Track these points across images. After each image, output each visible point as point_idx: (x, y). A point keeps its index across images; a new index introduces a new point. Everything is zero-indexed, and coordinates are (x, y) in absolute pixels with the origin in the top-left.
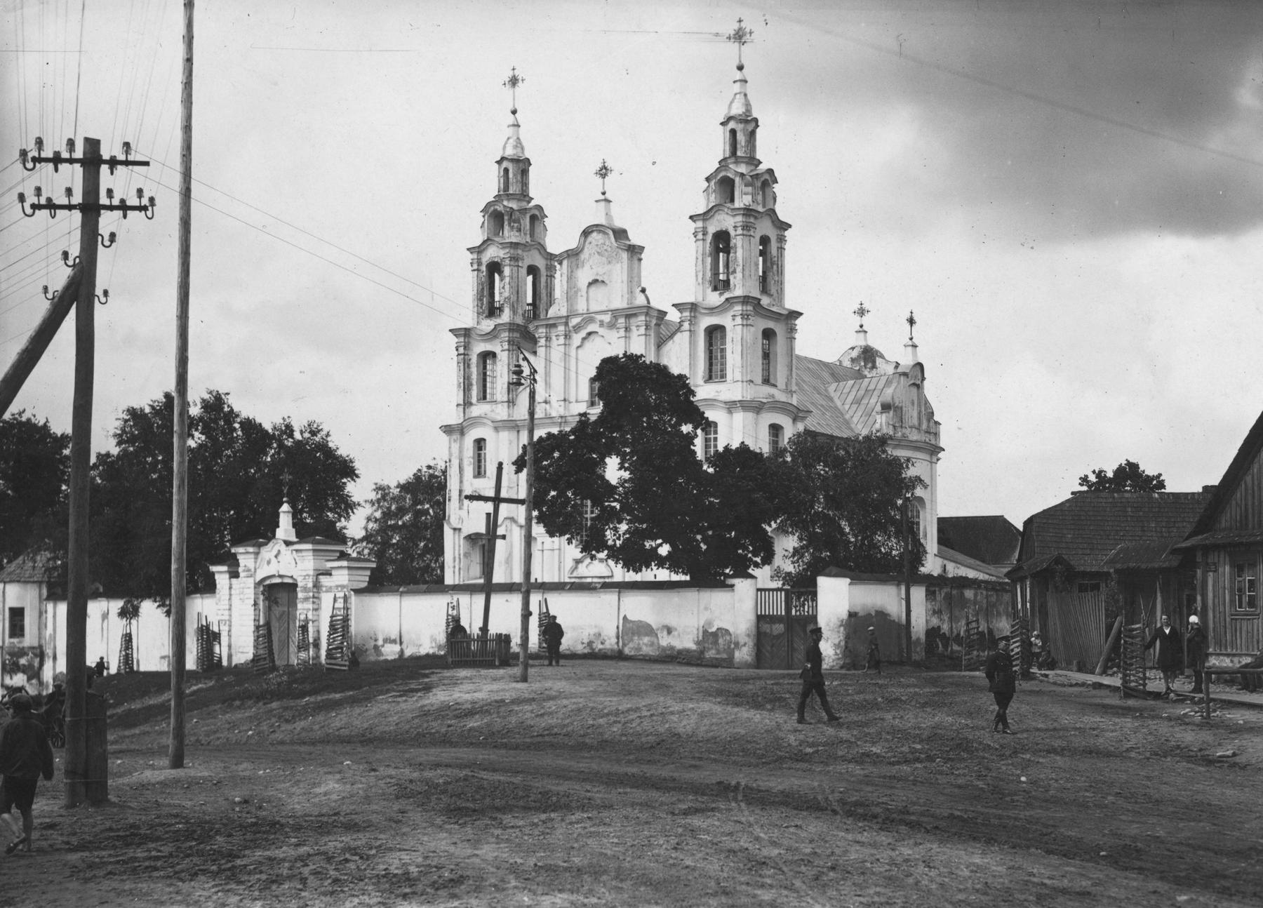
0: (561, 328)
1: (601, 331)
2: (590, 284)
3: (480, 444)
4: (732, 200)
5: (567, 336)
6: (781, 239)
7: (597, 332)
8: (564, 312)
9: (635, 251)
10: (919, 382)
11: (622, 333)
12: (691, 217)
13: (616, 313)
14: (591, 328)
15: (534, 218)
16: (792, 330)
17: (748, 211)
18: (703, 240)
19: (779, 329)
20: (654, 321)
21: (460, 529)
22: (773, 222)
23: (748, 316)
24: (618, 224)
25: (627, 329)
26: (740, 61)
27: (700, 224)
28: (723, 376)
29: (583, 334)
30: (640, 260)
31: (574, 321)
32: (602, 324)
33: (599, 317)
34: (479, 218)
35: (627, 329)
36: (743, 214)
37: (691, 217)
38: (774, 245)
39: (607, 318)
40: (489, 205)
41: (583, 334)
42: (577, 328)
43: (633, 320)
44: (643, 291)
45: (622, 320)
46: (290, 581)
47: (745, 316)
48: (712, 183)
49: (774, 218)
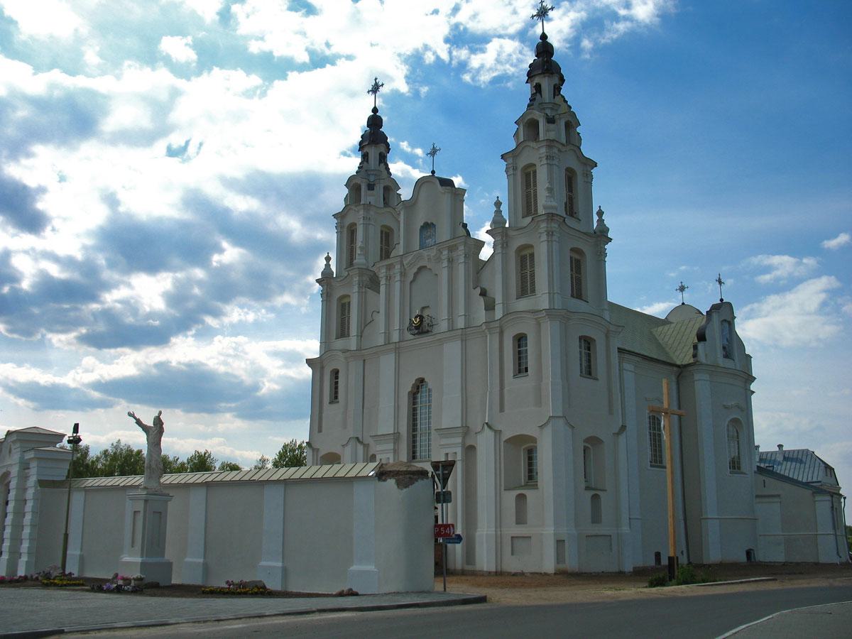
0: (398, 267)
5: (403, 274)
6: (589, 178)
7: (425, 267)
10: (729, 320)
11: (445, 264)
17: (551, 143)
21: (318, 449)
23: (552, 233)
25: (451, 261)
28: (533, 291)
38: (580, 179)
41: (415, 270)
47: (550, 234)
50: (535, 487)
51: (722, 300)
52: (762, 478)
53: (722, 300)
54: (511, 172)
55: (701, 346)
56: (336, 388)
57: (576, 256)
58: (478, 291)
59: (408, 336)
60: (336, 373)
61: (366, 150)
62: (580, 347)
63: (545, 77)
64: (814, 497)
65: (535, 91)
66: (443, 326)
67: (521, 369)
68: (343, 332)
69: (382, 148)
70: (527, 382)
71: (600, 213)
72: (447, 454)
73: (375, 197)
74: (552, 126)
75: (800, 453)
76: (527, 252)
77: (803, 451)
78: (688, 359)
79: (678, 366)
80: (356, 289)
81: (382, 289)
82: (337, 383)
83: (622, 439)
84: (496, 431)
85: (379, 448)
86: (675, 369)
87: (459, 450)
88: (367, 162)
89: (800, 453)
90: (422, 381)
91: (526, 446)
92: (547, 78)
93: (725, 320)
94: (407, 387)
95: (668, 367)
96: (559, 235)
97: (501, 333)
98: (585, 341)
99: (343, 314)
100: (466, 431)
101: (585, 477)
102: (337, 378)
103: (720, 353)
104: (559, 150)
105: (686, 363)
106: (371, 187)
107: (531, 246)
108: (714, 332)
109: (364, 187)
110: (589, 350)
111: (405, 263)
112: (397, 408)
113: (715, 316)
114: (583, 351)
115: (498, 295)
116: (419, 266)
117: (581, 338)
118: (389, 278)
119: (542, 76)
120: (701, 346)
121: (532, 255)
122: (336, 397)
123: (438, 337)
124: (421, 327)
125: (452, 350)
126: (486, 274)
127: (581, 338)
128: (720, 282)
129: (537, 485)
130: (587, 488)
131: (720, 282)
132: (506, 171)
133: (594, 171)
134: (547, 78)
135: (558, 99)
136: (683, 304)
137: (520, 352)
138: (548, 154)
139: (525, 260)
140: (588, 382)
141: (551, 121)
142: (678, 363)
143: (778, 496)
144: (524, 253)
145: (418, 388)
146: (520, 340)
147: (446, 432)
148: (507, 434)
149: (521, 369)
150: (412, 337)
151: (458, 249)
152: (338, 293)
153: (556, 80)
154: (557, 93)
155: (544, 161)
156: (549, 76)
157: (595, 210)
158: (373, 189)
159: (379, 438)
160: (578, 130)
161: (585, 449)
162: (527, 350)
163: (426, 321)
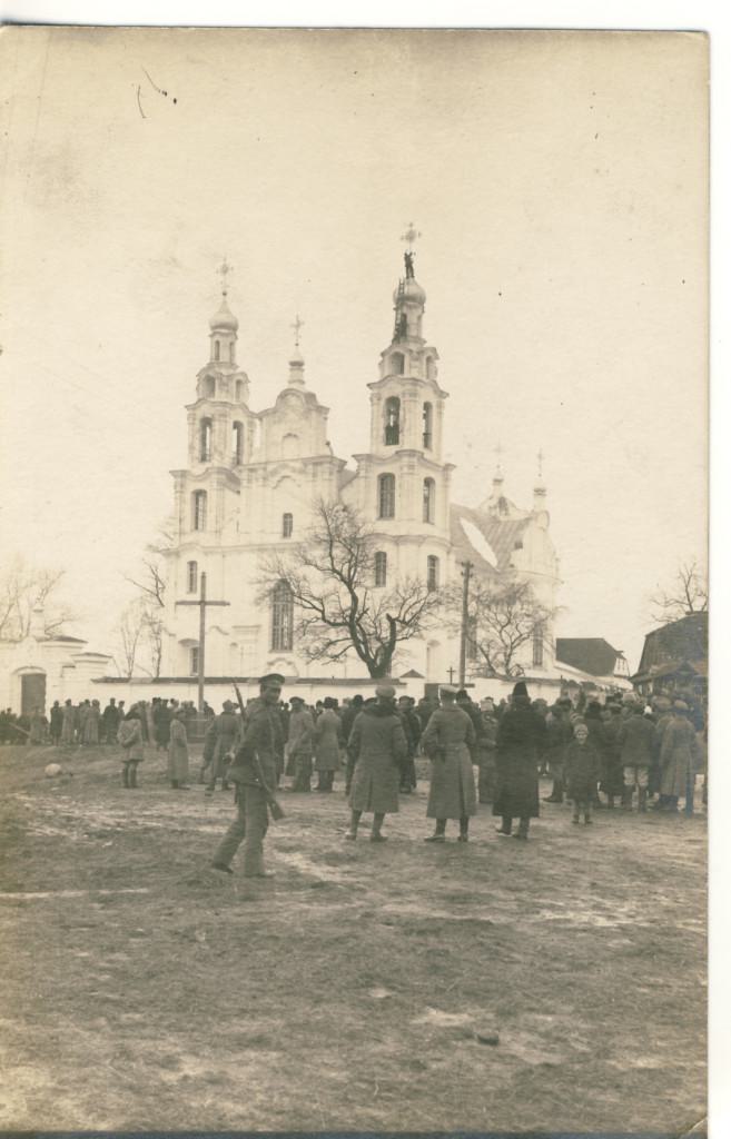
0: (261, 472)
1: (294, 475)
2: (285, 437)
3: (192, 564)
4: (402, 371)
6: (440, 406)
7: (288, 477)
8: (263, 459)
9: (322, 410)
10: (545, 527)
12: (368, 385)
13: (305, 462)
14: (286, 472)
15: (239, 382)
16: (446, 479)
20: (337, 469)
24: (308, 388)
25: (314, 475)
27: (376, 391)
29: (277, 478)
30: (326, 419)
31: (270, 468)
32: (294, 470)
33: (292, 464)
34: (194, 382)
35: (314, 475)
37: (368, 385)
38: (434, 411)
39: (298, 465)
40: (204, 370)
41: (277, 478)
42: (274, 473)
43: (319, 468)
44: (328, 444)
45: (310, 467)
46: (38, 671)
48: (387, 357)
54: (375, 400)
118: (249, 481)
152: (192, 486)
155: (407, 398)
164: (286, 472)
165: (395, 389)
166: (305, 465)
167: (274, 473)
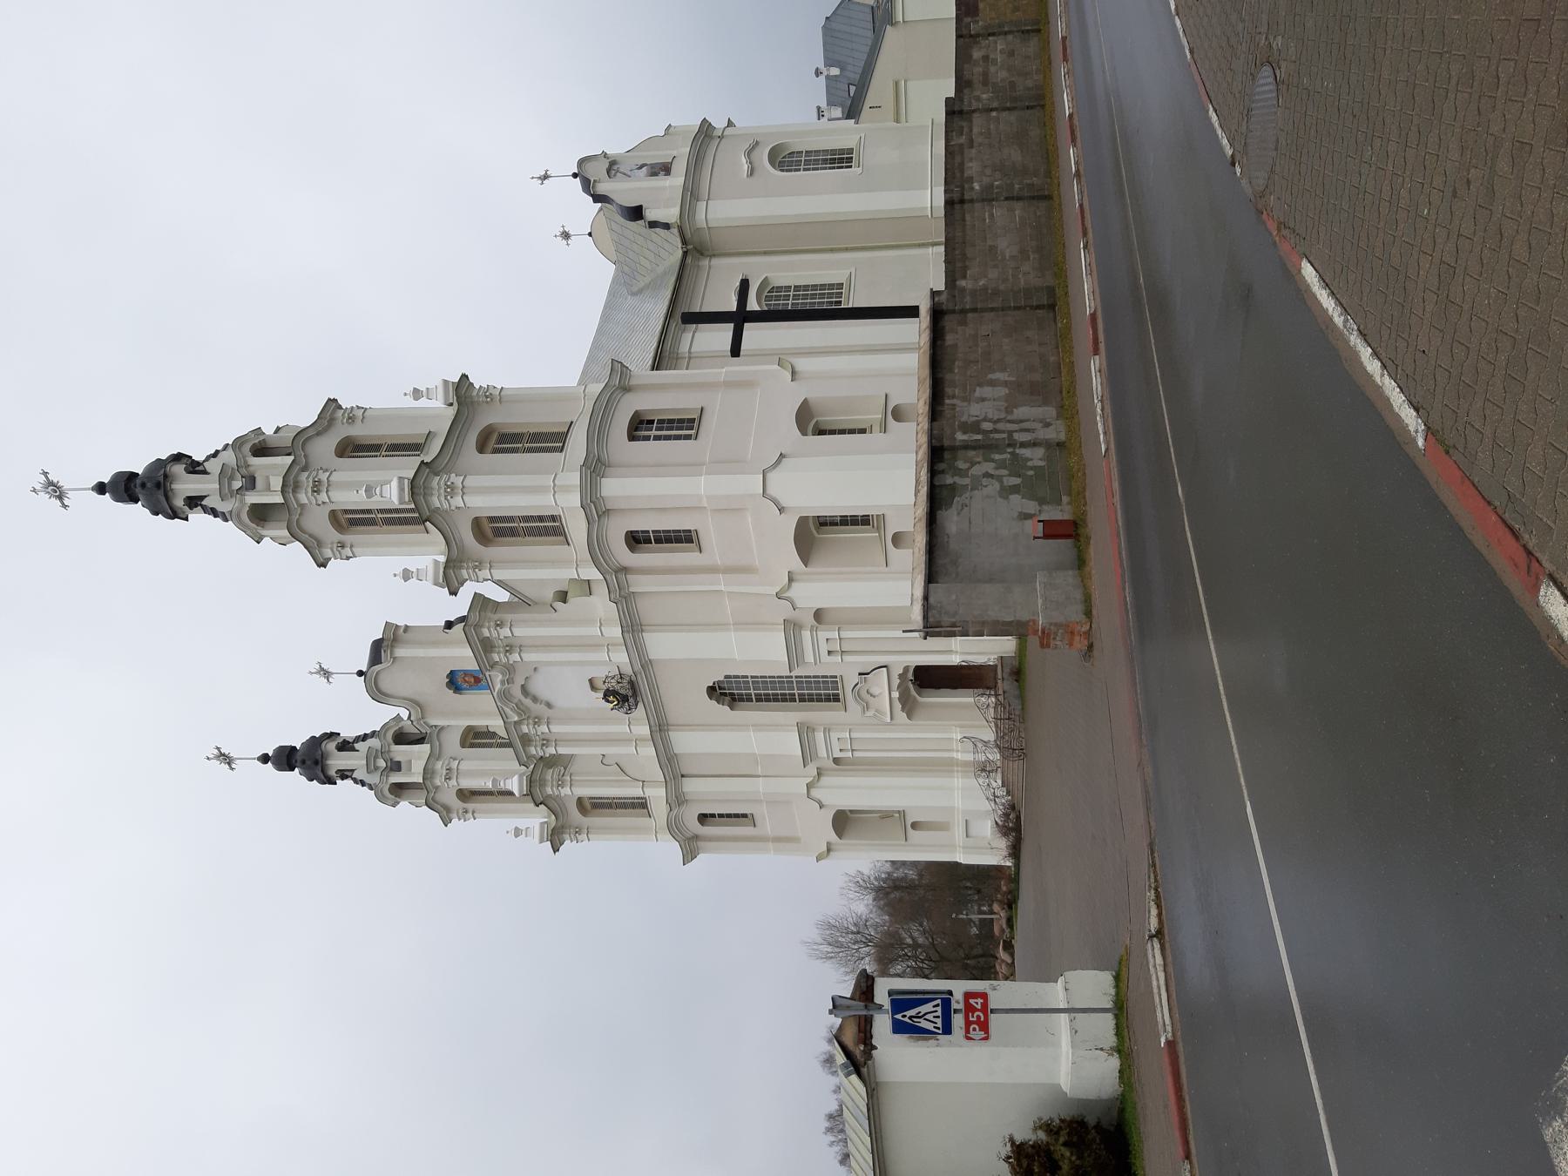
0: (525, 729)
1: (519, 681)
5: (537, 721)
11: (515, 657)
14: (516, 691)
18: (351, 546)
19: (486, 419)
22: (318, 434)
23: (448, 487)
25: (509, 649)
26: (89, 489)
28: (553, 518)
29: (528, 702)
30: (407, 628)
36: (294, 491)
38: (358, 431)
40: (381, 797)
41: (528, 702)
47: (451, 490)
48: (264, 532)
49: (311, 432)
50: (882, 518)
51: (575, 175)
52: (866, 110)
53: (575, 175)
54: (348, 551)
55: (651, 214)
56: (729, 816)
57: (492, 444)
58: (558, 605)
59: (640, 712)
60: (703, 818)
61: (332, 773)
62: (647, 438)
63: (172, 490)
64: (897, 23)
65: (199, 507)
66: (621, 658)
67: (684, 538)
68: (641, 805)
69: (331, 746)
70: (710, 533)
71: (417, 394)
72: (830, 653)
73: (415, 757)
74: (259, 483)
75: (673, 366)
76: (487, 527)
77: (825, 35)
78: (674, 237)
79: (685, 254)
80: (566, 791)
81: (562, 750)
82: (721, 816)
83: (802, 364)
84: (791, 580)
85: (822, 752)
86: (689, 260)
87: (823, 635)
88: (353, 771)
89: (673, 366)
90: (712, 691)
91: (815, 532)
92: (173, 486)
93: (608, 172)
94: (721, 711)
95: (687, 272)
96: (453, 475)
97: (625, 570)
98: (637, 429)
99: (609, 806)
100: (792, 628)
101: (863, 431)
102: (713, 816)
103: (662, 182)
104: (305, 469)
105: (679, 240)
106: (396, 767)
107: (477, 522)
108: (626, 191)
109: (397, 778)
110: (652, 422)
111: (516, 719)
112: (758, 727)
113: (602, 188)
114: (654, 433)
115: (563, 575)
116: (522, 698)
117: (632, 438)
119: (170, 493)
120: (651, 214)
121: (492, 519)
122: (745, 816)
123: (638, 667)
124: (623, 694)
125: (660, 645)
126: (530, 592)
127: (632, 438)
128: (546, 177)
129: (877, 515)
130: (884, 429)
131: (546, 177)
132: (348, 558)
133: (345, 403)
134: (173, 486)
135: (214, 467)
136: (590, 234)
137: (658, 541)
138: (310, 490)
139: (494, 530)
140: (709, 426)
141: (251, 483)
142: (680, 253)
143: (897, 84)
144: (489, 533)
145: (725, 694)
146: (636, 540)
147: (794, 652)
148: (795, 562)
149: (684, 538)
150: (640, 705)
151: (488, 638)
153: (179, 469)
154: (201, 468)
155: (323, 497)
156: (171, 483)
157: (410, 403)
158: (399, 762)
159: (808, 753)
160: (269, 430)
161: (822, 432)
162: (653, 531)
163: (613, 684)
164: (516, 691)
165: (318, 522)
166: (493, 665)
167: (520, 709)
